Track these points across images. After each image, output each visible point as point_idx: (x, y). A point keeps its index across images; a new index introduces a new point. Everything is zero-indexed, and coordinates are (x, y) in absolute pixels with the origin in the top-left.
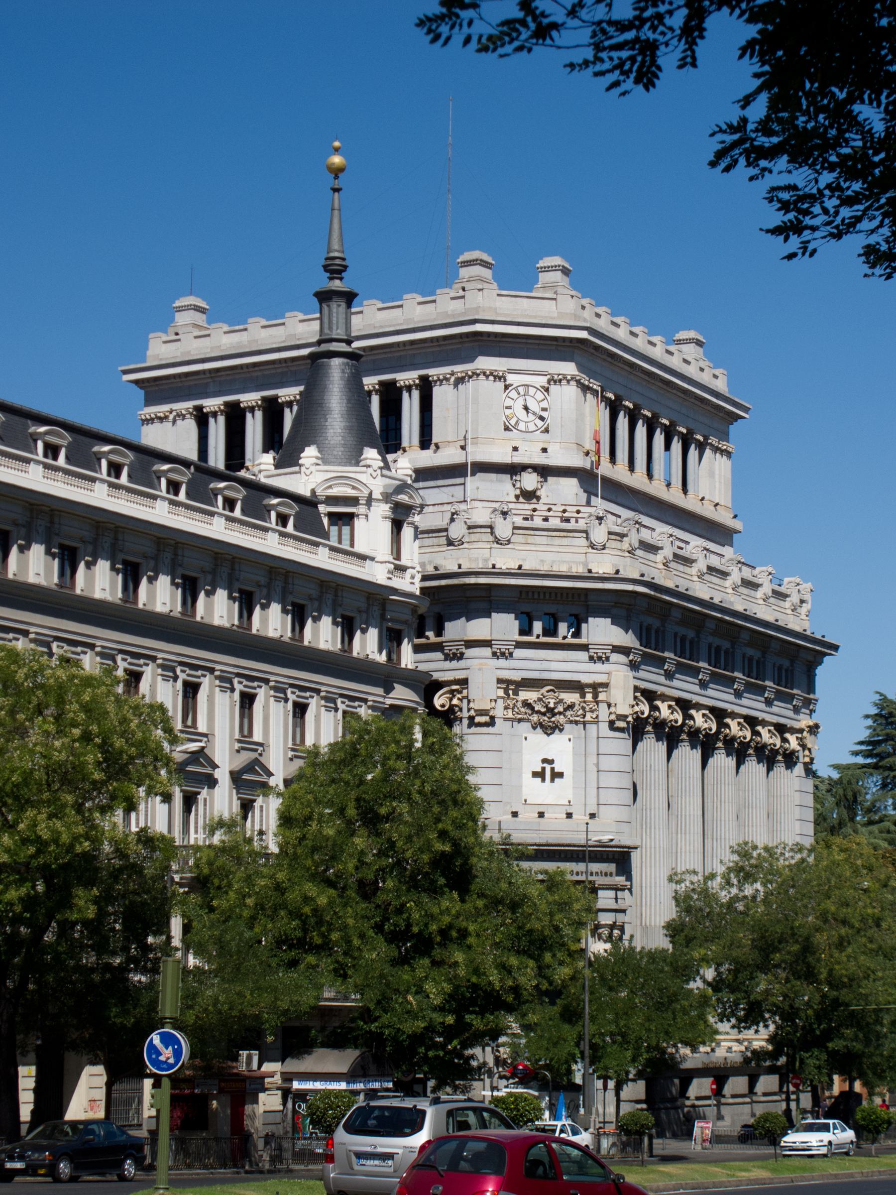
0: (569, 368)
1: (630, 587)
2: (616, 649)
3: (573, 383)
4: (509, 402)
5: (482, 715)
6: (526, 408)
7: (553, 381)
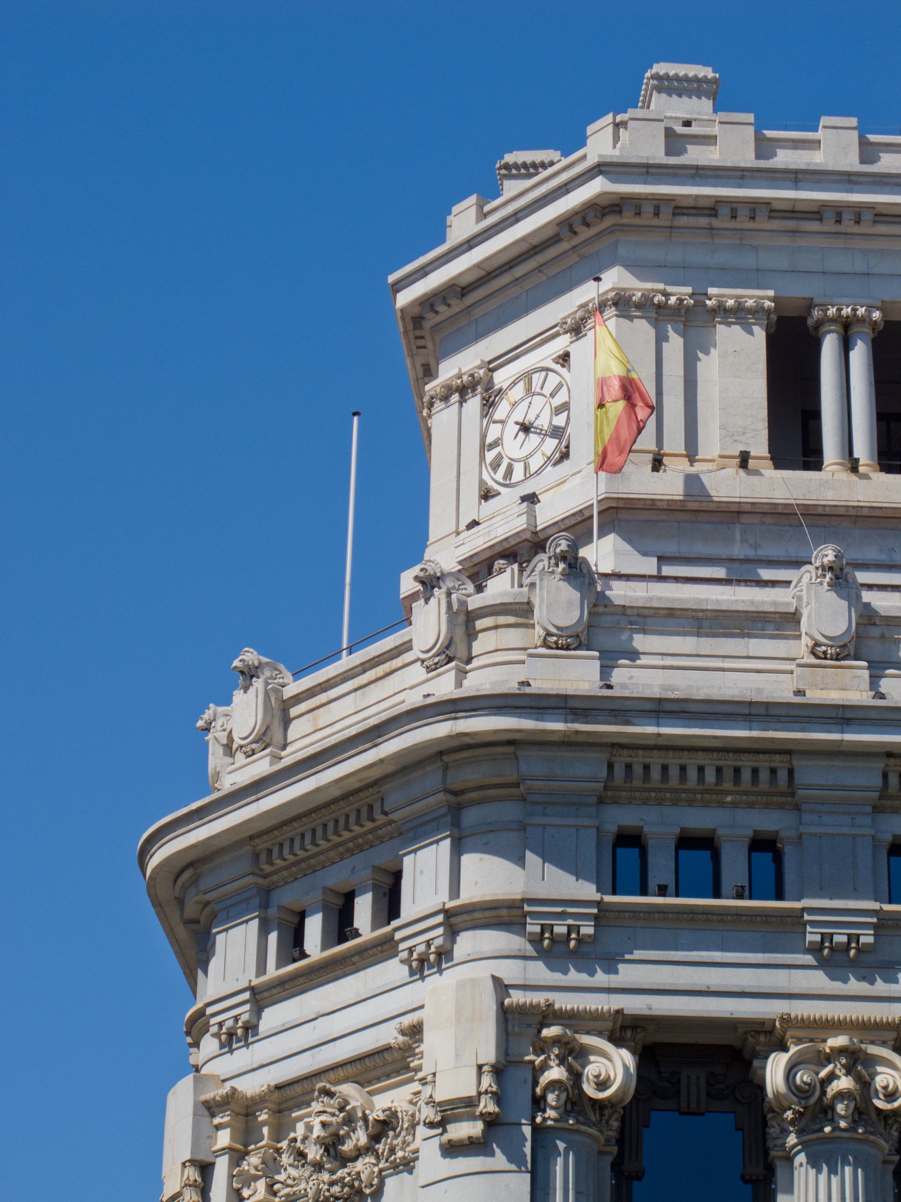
1: (440, 730)
3: (611, 312)
4: (494, 432)
6: (526, 428)
7: (577, 330)
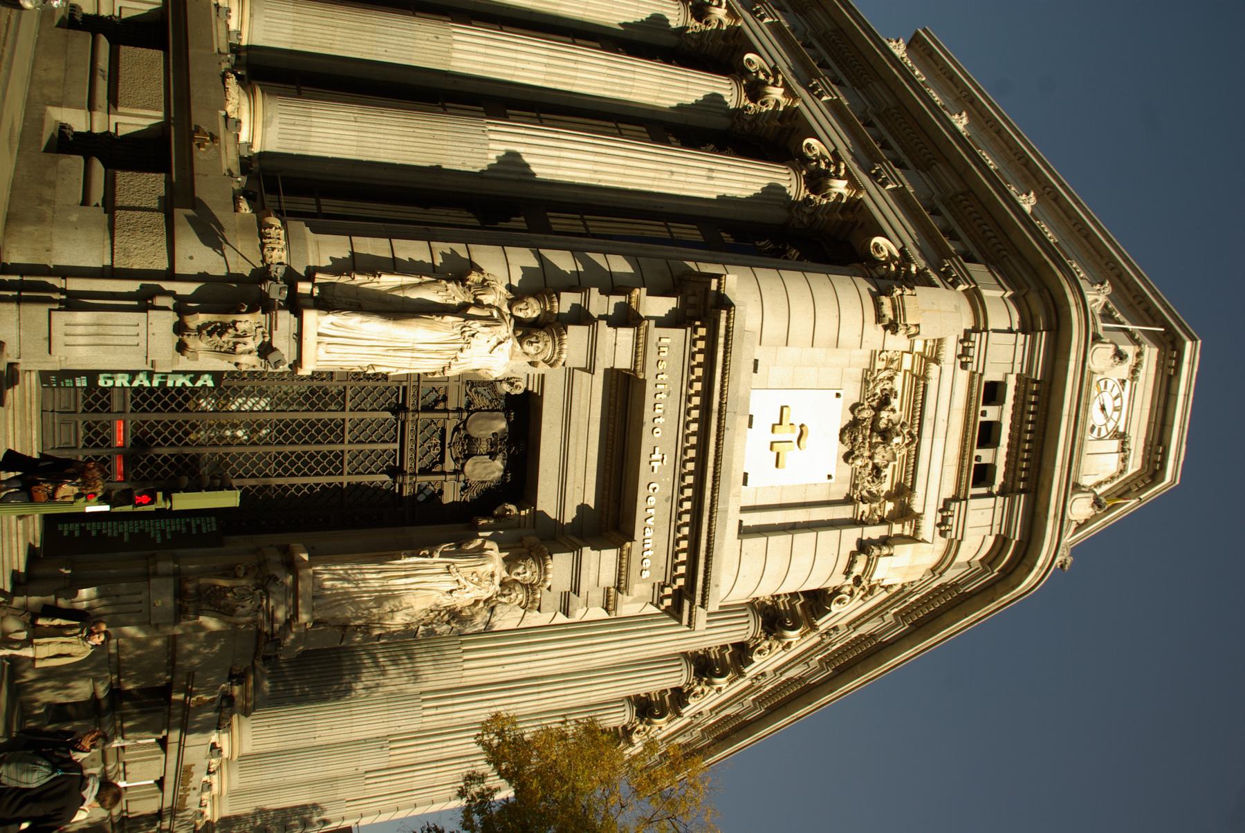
0: (1135, 464)
2: (954, 546)
5: (894, 309)
6: (1103, 408)
